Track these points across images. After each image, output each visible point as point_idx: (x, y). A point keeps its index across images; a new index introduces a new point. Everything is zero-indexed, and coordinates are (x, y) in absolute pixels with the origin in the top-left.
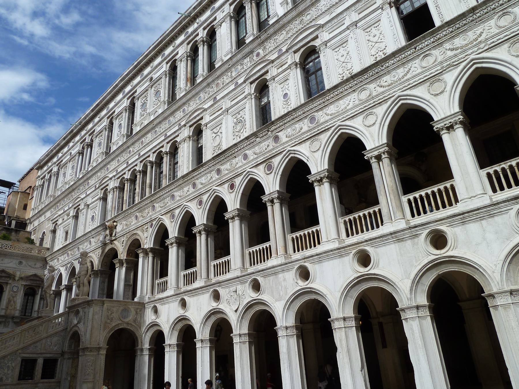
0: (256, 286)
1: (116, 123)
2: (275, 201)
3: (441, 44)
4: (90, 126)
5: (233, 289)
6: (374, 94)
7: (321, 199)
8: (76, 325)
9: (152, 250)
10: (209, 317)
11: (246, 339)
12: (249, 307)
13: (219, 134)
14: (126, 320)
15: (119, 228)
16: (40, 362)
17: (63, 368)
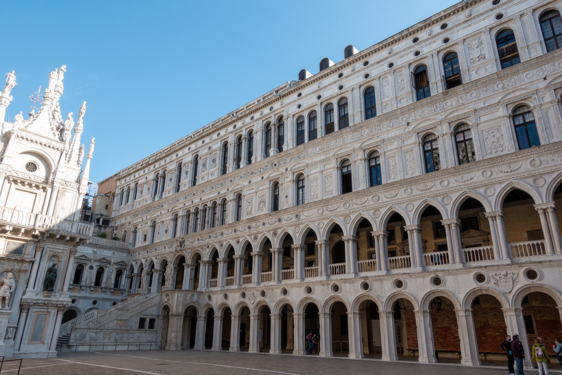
4: (162, 162)
5: (252, 293)
8: (166, 302)
9: (208, 262)
12: (259, 303)
14: (194, 301)
15: (187, 243)
16: (148, 320)
17: (159, 323)
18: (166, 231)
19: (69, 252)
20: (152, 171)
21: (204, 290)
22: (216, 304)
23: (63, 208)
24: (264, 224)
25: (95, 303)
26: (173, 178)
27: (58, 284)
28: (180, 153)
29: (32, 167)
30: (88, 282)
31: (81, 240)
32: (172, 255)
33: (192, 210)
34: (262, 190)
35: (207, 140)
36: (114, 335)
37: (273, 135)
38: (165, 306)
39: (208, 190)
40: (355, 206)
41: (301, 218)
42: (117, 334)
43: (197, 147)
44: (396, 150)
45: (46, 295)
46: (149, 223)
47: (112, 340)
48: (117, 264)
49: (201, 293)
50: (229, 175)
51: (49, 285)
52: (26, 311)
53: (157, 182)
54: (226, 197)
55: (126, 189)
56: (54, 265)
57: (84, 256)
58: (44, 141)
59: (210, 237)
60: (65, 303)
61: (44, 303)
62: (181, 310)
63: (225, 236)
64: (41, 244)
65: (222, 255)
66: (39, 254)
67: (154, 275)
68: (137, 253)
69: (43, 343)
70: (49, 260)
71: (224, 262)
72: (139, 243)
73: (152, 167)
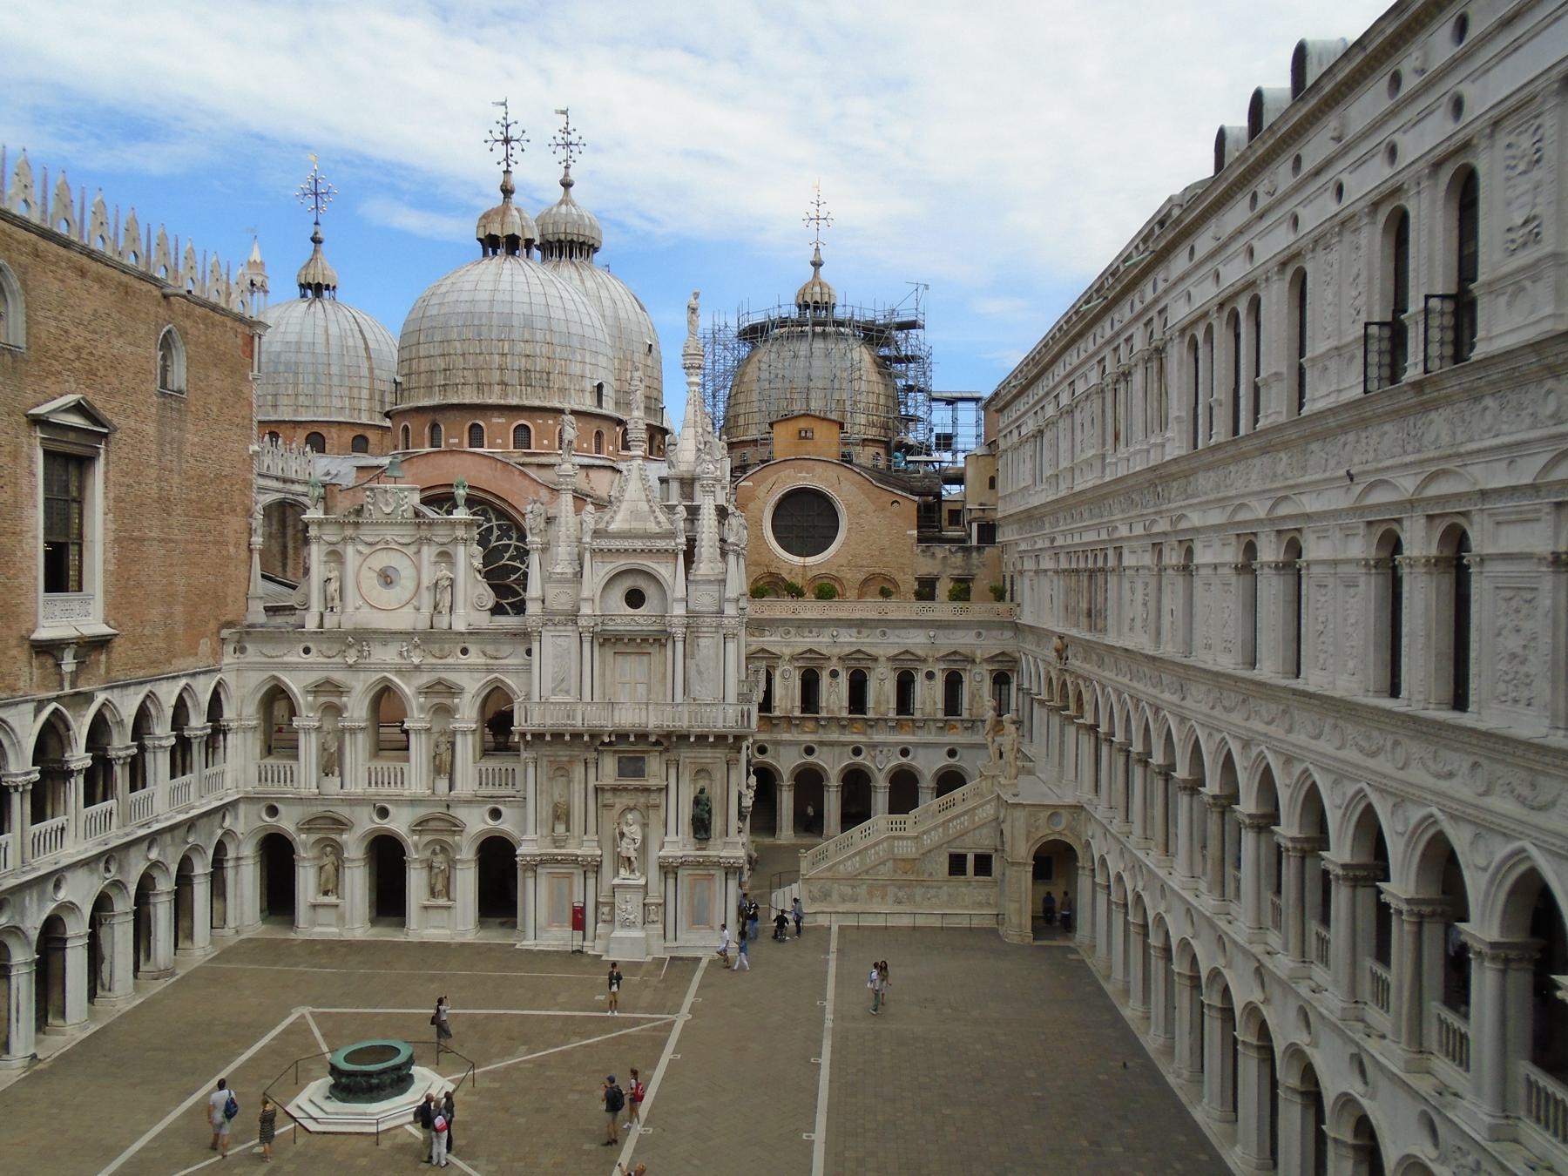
14: (1059, 828)
23: (700, 672)
25: (952, 753)
27: (717, 823)
29: (635, 598)
30: (928, 709)
36: (891, 890)
47: (890, 899)
48: (991, 660)
51: (701, 826)
56: (702, 791)
57: (907, 652)
58: (639, 544)
64: (672, 755)
66: (673, 772)
69: (712, 928)
70: (695, 781)
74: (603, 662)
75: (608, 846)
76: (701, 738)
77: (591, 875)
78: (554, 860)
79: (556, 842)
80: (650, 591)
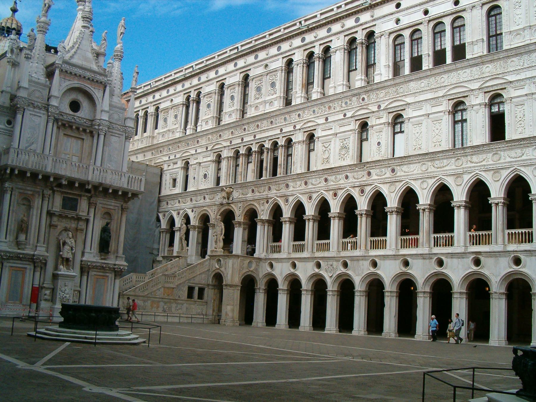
0: (345, 265)
1: (227, 93)
2: (363, 215)
3: (467, 156)
4: (195, 81)
5: (331, 263)
6: (429, 170)
7: (390, 224)
9: (268, 221)
10: (312, 277)
11: (336, 293)
12: (339, 276)
13: (328, 149)
14: (251, 269)
15: (236, 195)
16: (197, 289)
17: (209, 294)
18: (205, 176)
19: (120, 208)
20: (181, 91)
21: (263, 256)
22: (281, 274)
24: (347, 177)
26: (212, 105)
27: (112, 246)
28: (222, 70)
29: (75, 106)
31: (133, 194)
32: (215, 208)
33: (242, 151)
34: (345, 132)
35: (262, 55)
36: (162, 304)
37: (359, 57)
38: (216, 274)
39: (265, 125)
40: (470, 165)
41: (398, 174)
42: (165, 303)
43: (248, 63)
44: (525, 98)
45: (103, 257)
46: (180, 164)
47: (160, 309)
49: (260, 259)
50: (293, 109)
51: (104, 246)
52: (86, 274)
53: (188, 107)
54: (292, 137)
55: (141, 114)
56: (108, 224)
58: (88, 74)
59: (270, 189)
60: (122, 267)
61: (103, 267)
62: (237, 280)
63: (291, 189)
65: (287, 213)
66: (92, 210)
67: (191, 233)
68: (165, 203)
71: (291, 222)
72: (167, 190)
73: (179, 87)
74: (57, 139)
75: (53, 249)
76: (115, 192)
77: (39, 269)
78: (18, 257)
79: (18, 244)
80: (85, 104)
